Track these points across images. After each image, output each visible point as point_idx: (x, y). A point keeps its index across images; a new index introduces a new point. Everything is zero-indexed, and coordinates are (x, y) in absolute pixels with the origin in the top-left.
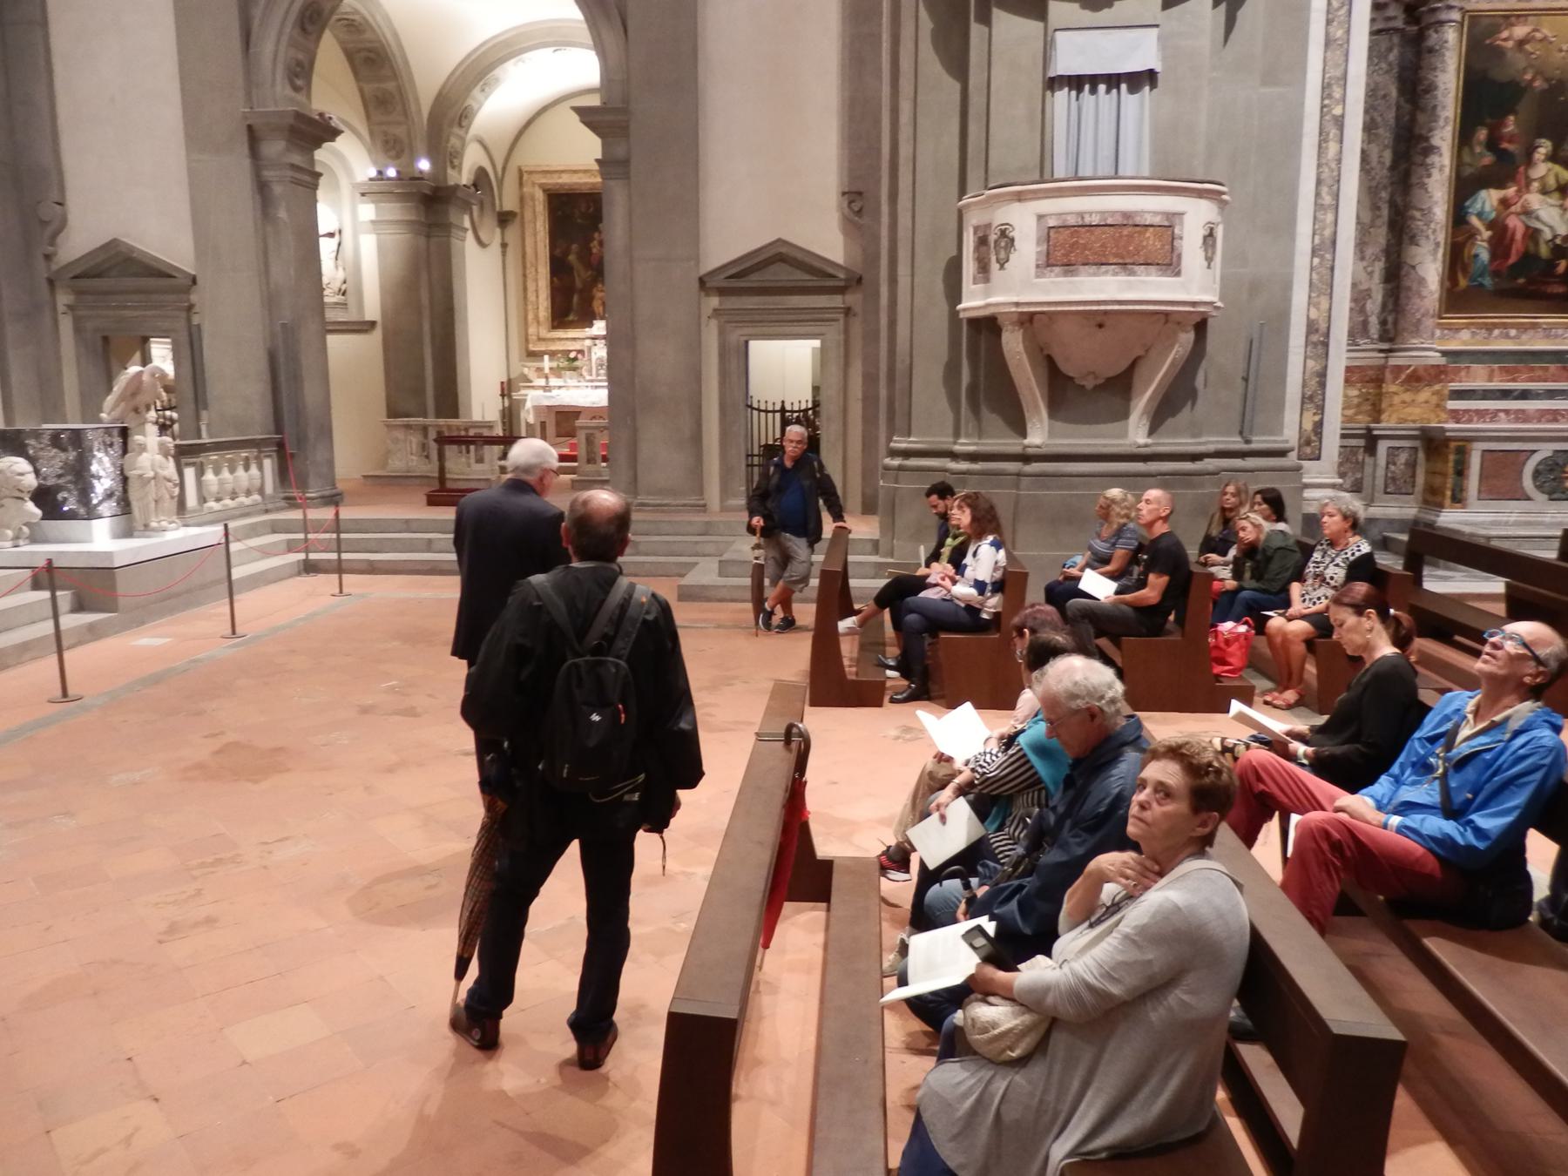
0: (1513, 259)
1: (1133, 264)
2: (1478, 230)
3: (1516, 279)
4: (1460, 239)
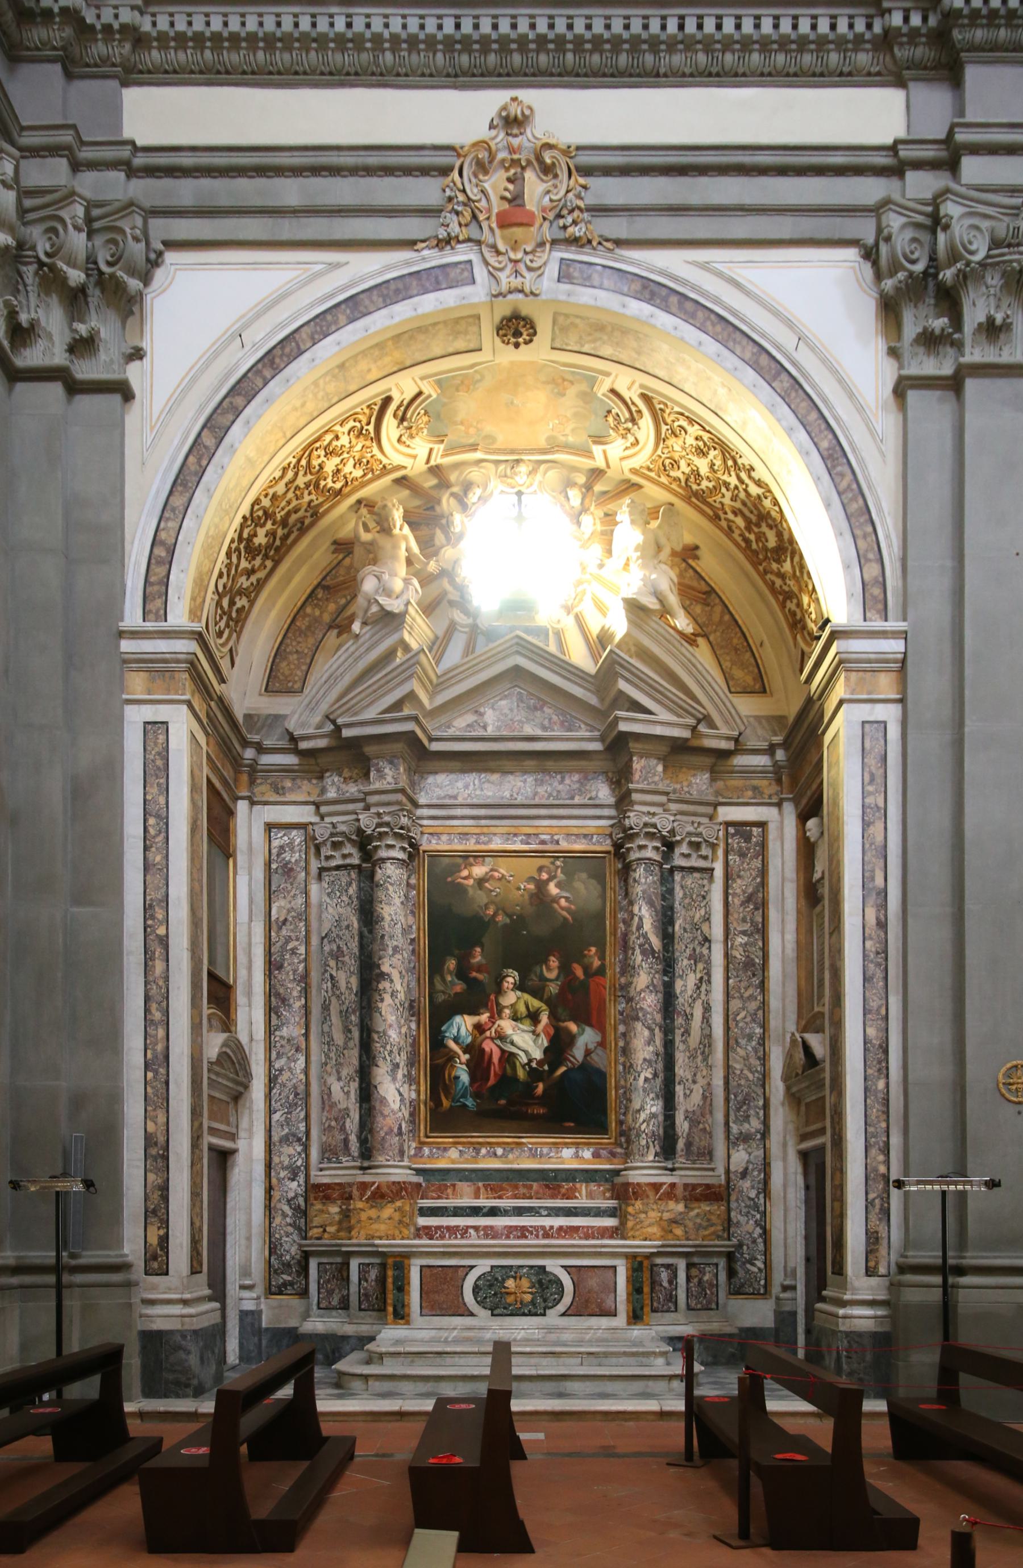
0: (492, 1081)
2: (456, 1053)
4: (440, 1061)
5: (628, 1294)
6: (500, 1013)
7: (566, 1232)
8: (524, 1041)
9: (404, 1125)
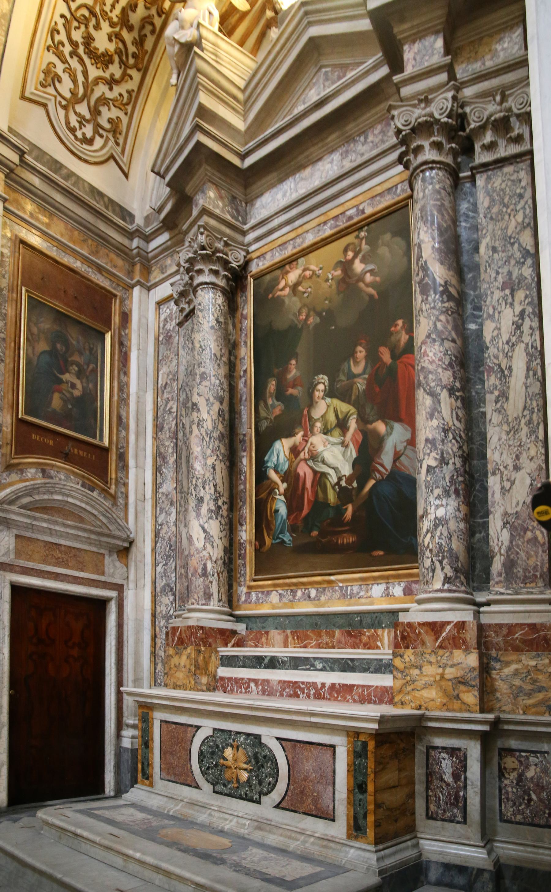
3: (311, 531)
5: (349, 791)
6: (312, 426)
7: (338, 693)
8: (335, 457)
9: (209, 565)
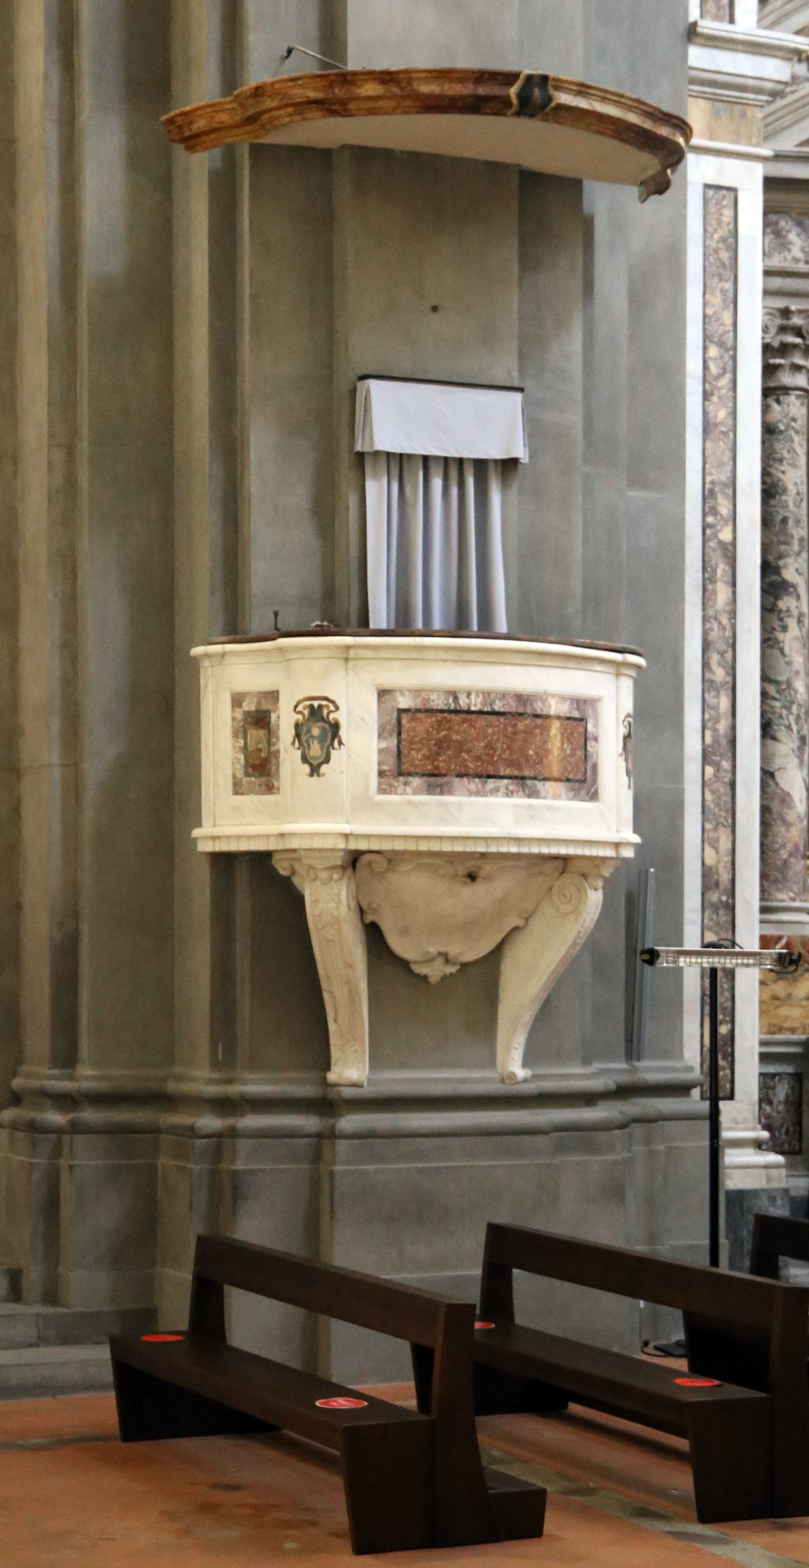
1: (535, 778)
